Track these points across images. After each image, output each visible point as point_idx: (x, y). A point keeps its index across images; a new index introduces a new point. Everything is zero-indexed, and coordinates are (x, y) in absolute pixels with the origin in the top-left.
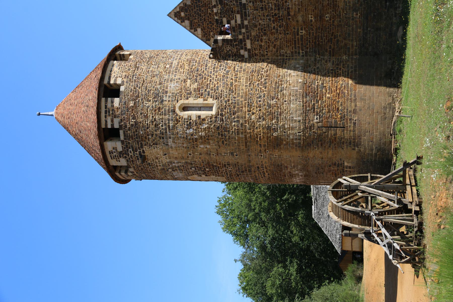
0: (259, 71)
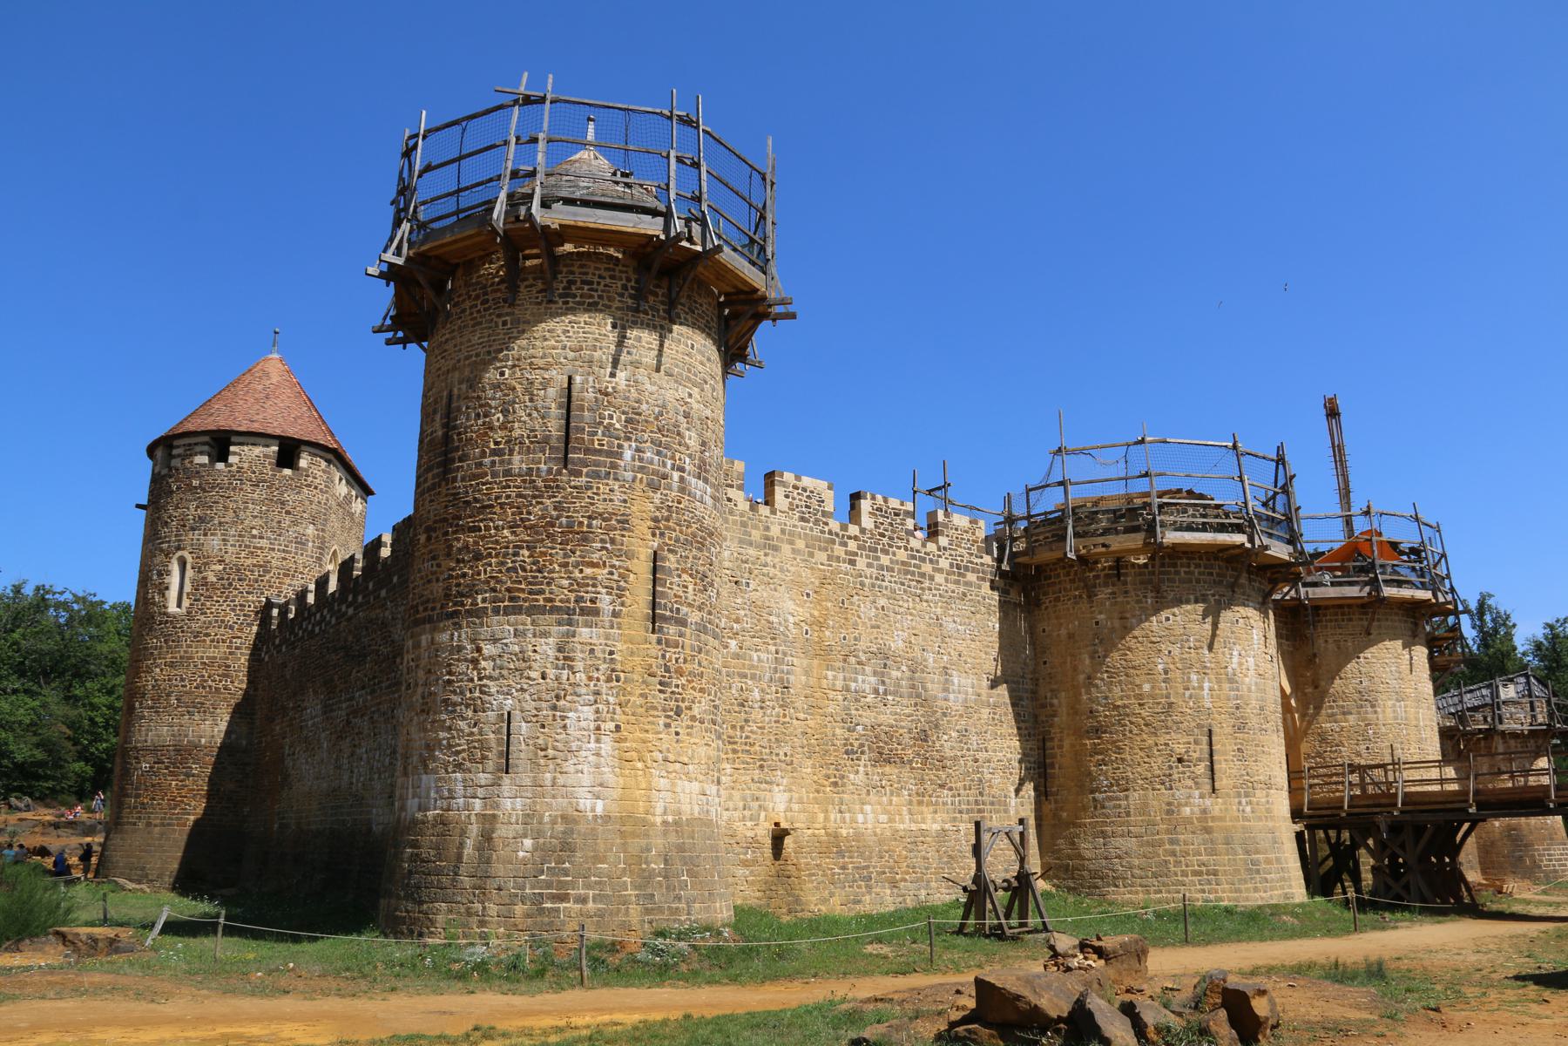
0: (227, 676)
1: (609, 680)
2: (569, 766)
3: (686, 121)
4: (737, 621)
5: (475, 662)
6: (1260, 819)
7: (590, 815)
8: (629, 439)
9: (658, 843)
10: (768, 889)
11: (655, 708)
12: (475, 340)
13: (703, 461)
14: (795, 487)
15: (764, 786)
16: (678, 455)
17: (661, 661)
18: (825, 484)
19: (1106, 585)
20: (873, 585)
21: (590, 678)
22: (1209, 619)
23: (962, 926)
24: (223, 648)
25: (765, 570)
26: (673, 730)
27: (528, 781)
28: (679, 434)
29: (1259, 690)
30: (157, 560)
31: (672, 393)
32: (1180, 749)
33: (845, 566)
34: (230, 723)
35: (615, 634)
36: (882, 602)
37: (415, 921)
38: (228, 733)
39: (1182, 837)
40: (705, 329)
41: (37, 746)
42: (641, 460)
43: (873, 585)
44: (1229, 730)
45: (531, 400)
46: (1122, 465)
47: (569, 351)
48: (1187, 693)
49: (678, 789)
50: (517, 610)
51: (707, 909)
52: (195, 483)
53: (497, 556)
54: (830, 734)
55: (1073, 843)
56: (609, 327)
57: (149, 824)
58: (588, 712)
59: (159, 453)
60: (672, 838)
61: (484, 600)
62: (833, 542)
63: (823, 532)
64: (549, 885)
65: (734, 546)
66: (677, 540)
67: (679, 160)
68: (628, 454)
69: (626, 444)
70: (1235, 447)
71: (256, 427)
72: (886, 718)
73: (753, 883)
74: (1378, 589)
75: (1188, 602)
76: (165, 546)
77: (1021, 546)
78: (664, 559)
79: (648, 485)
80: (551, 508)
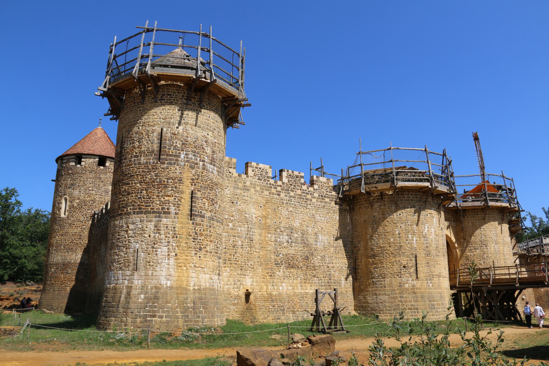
1: (173, 237)
2: (158, 269)
3: (206, 36)
4: (232, 216)
5: (127, 231)
6: (435, 289)
7: (165, 286)
8: (183, 150)
9: (191, 297)
10: (243, 314)
11: (191, 248)
12: (131, 117)
13: (213, 158)
14: (256, 168)
15: (242, 276)
16: (202, 156)
17: (193, 231)
18: (268, 166)
19: (377, 202)
20: (287, 203)
21: (166, 237)
22: (417, 214)
23: (312, 329)
24: (79, 229)
25: (244, 198)
26: (198, 256)
27: (143, 274)
28: (203, 148)
29: (436, 240)
30: (58, 199)
31: (200, 133)
32: (404, 263)
33: (276, 196)
34: (83, 256)
35: (177, 221)
36: (291, 209)
37: (105, 324)
38: (82, 259)
39: (405, 295)
40: (215, 111)
41: (36, 264)
42: (187, 158)
43: (287, 203)
44: (424, 255)
45: (148, 137)
46: (383, 157)
47: (162, 119)
48: (407, 242)
49: (200, 277)
50: (141, 213)
51: (211, 321)
52: (70, 172)
53: (135, 193)
54: (269, 257)
55: (365, 298)
56: (177, 111)
57: (54, 290)
58: (165, 249)
59: (59, 162)
60: (197, 295)
61: (130, 209)
62: (271, 187)
63: (267, 184)
64: (149, 311)
65: (232, 189)
66: (201, 187)
67: (202, 49)
68: (182, 156)
69: (182, 152)
70: (425, 150)
71: (91, 152)
72: (292, 251)
73: (237, 312)
74: (487, 203)
75: (408, 208)
76: (60, 194)
77: (346, 188)
78: (195, 194)
79: (190, 167)
80: (154, 176)
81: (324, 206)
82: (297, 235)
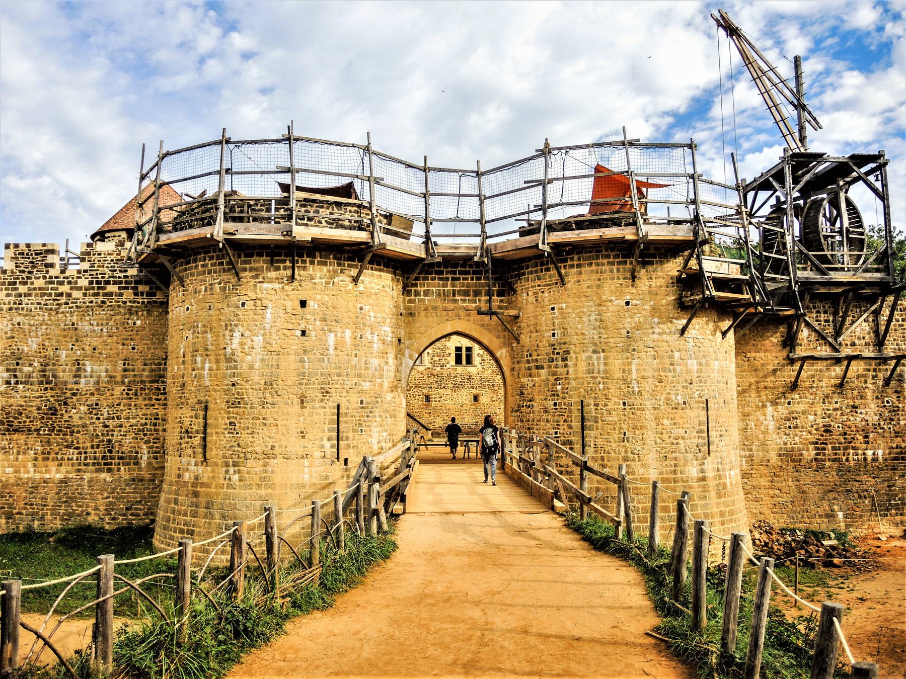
6: (249, 487)
36: (19, 319)
48: (194, 373)
81: (103, 302)
82: (31, 369)
